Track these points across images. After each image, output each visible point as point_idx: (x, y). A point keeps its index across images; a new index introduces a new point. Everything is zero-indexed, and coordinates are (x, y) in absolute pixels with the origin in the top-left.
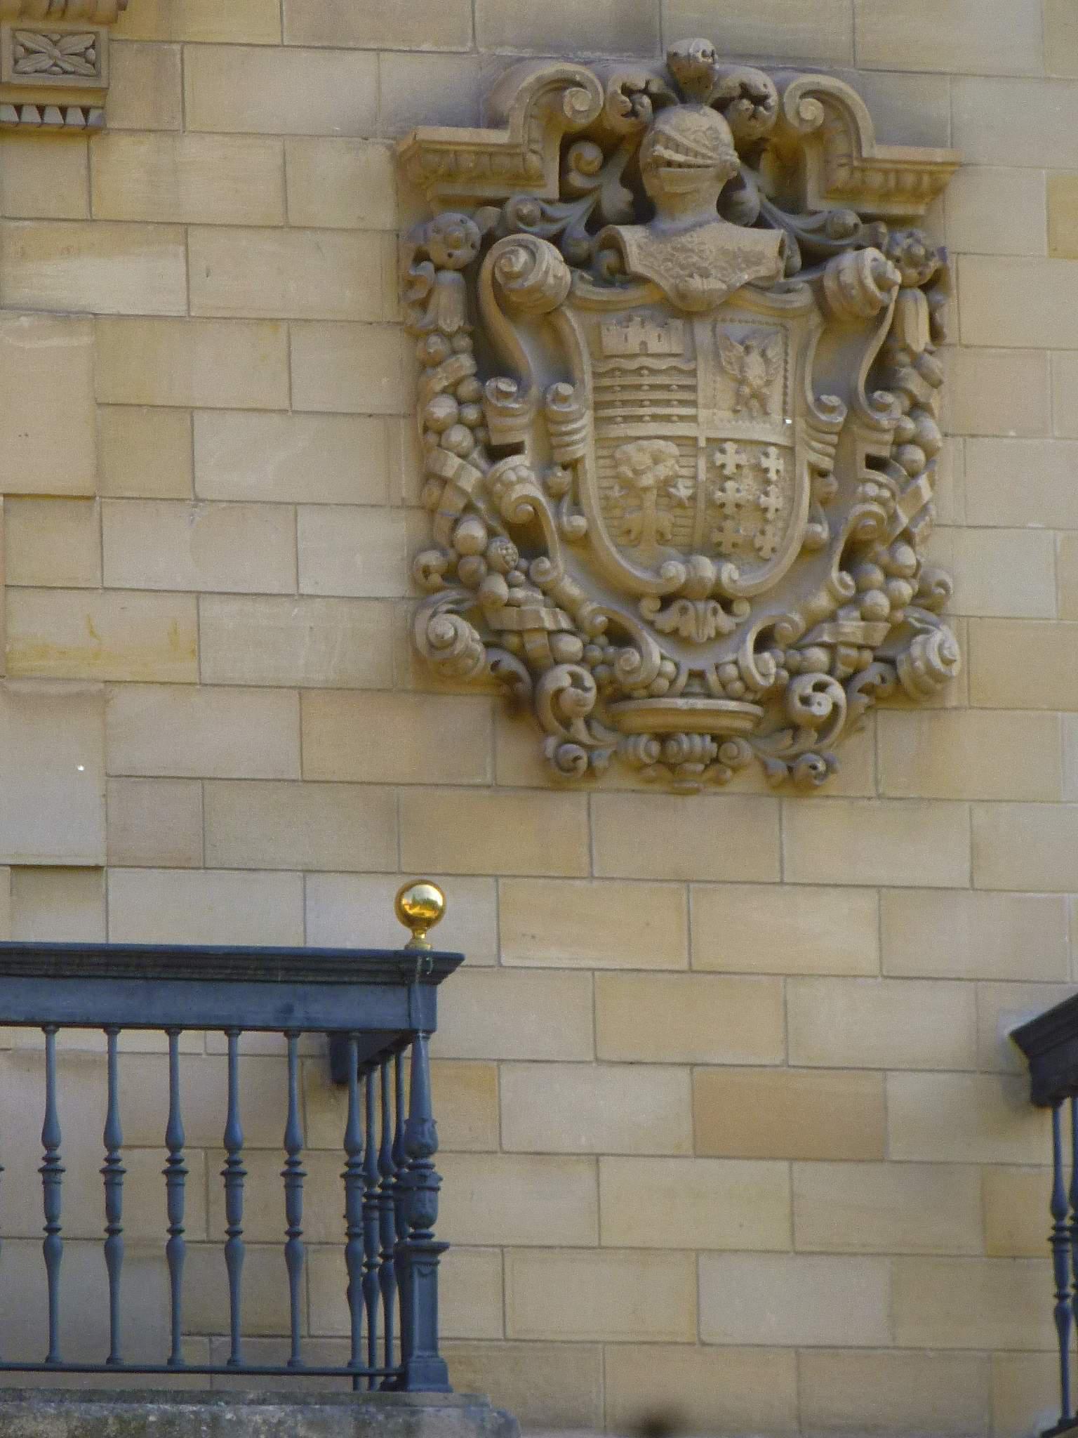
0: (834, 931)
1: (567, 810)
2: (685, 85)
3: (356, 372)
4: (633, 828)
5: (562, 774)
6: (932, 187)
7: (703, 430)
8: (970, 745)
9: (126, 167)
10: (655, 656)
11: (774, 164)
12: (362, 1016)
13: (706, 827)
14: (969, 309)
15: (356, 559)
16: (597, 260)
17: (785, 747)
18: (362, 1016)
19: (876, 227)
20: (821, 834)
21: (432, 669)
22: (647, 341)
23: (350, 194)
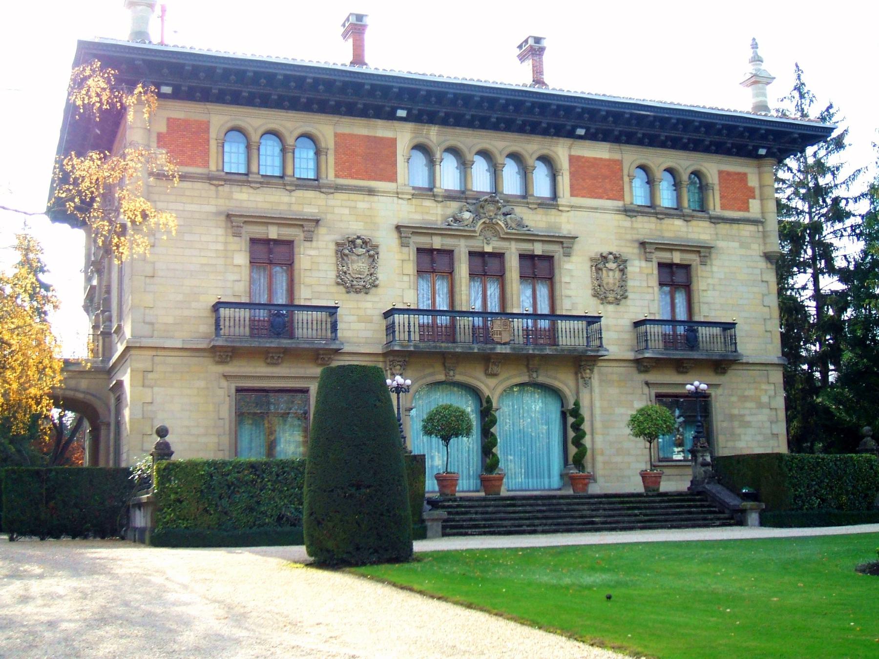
0: (369, 305)
1: (348, 295)
2: (359, 237)
3: (333, 260)
4: (353, 295)
5: (348, 292)
6: (377, 246)
7: (358, 265)
8: (379, 290)
9: (314, 244)
10: (355, 283)
11: (365, 243)
12: (332, 311)
13: (361, 296)
14: (381, 255)
15: (332, 275)
16: (351, 251)
17: (365, 290)
18: (332, 311)
19: (373, 249)
20: (368, 297)
21: (338, 284)
22: (355, 258)
23: (333, 247)
